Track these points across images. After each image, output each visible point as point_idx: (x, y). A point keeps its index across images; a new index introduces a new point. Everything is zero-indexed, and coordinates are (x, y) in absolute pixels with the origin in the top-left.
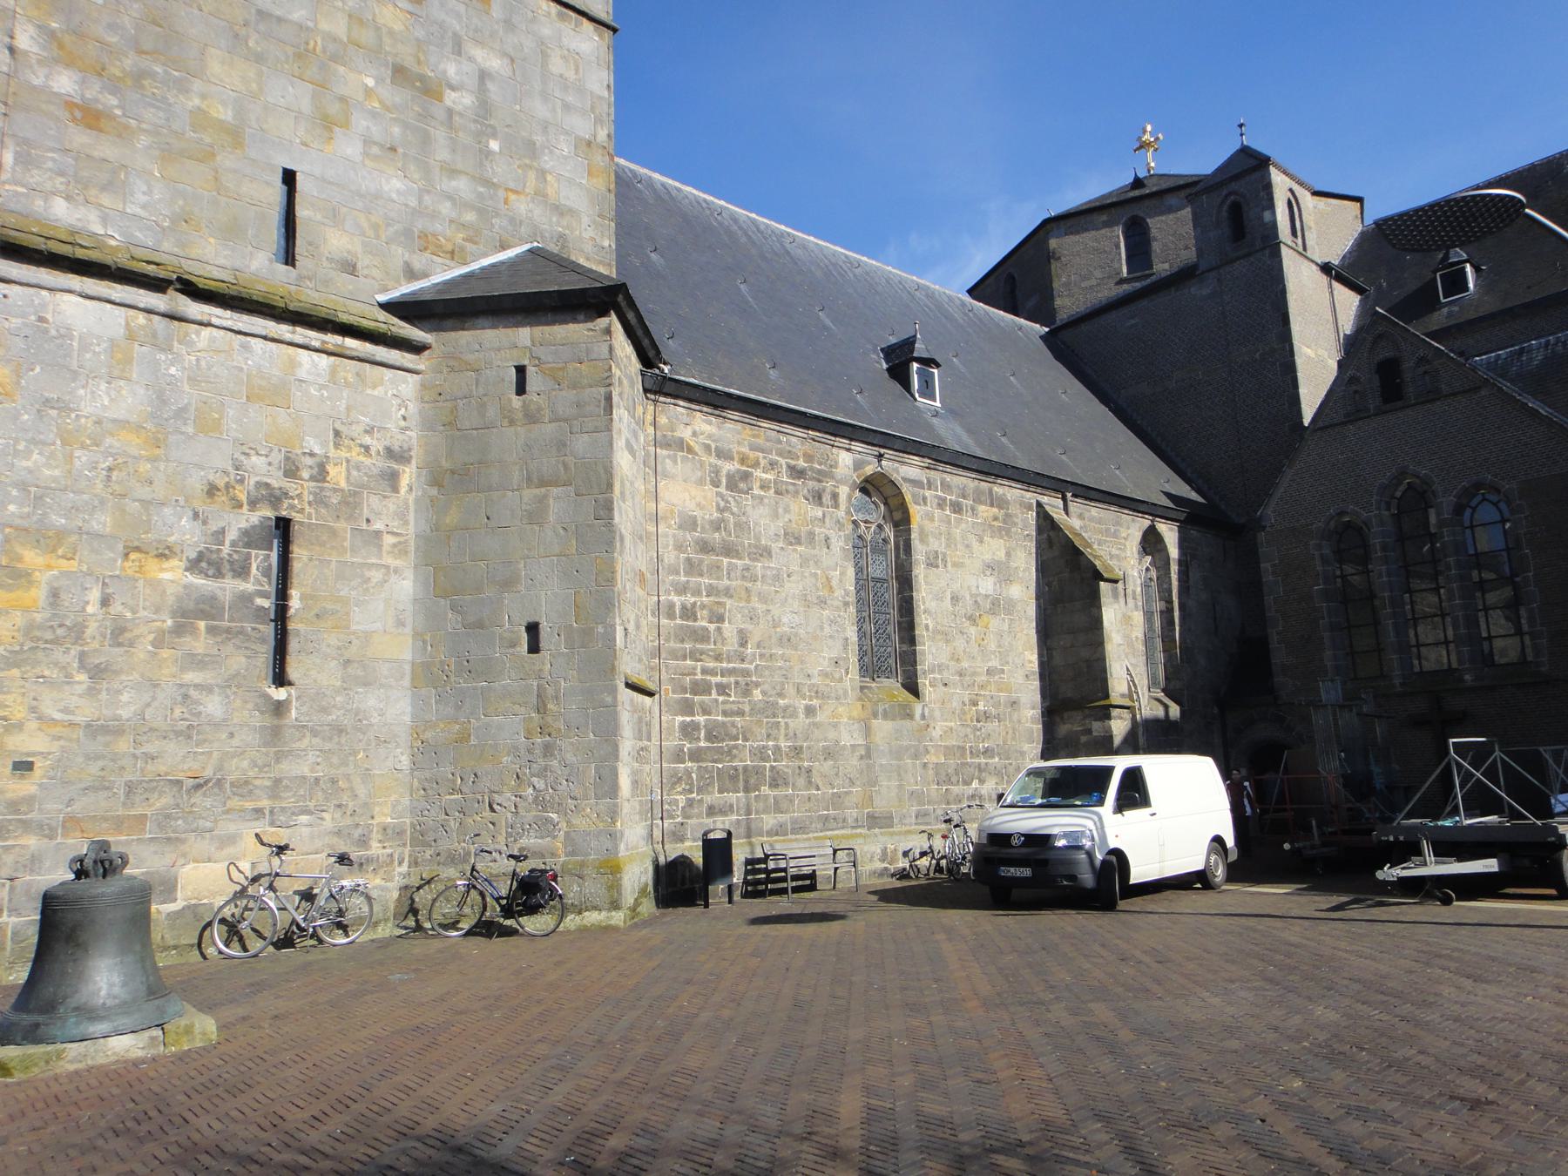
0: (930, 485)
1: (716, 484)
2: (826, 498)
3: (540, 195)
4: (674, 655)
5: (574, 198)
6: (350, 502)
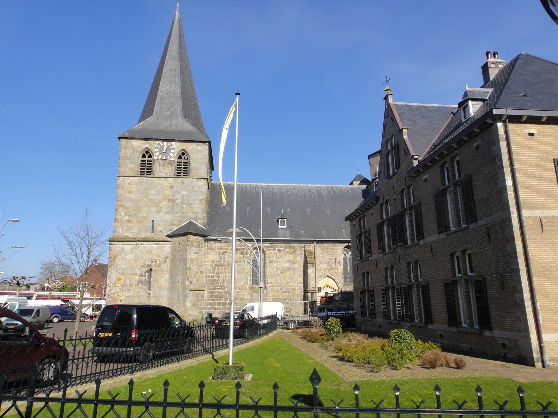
0: (271, 247)
1: (219, 254)
2: (245, 253)
3: (192, 211)
4: (209, 284)
5: (198, 210)
6: (160, 265)
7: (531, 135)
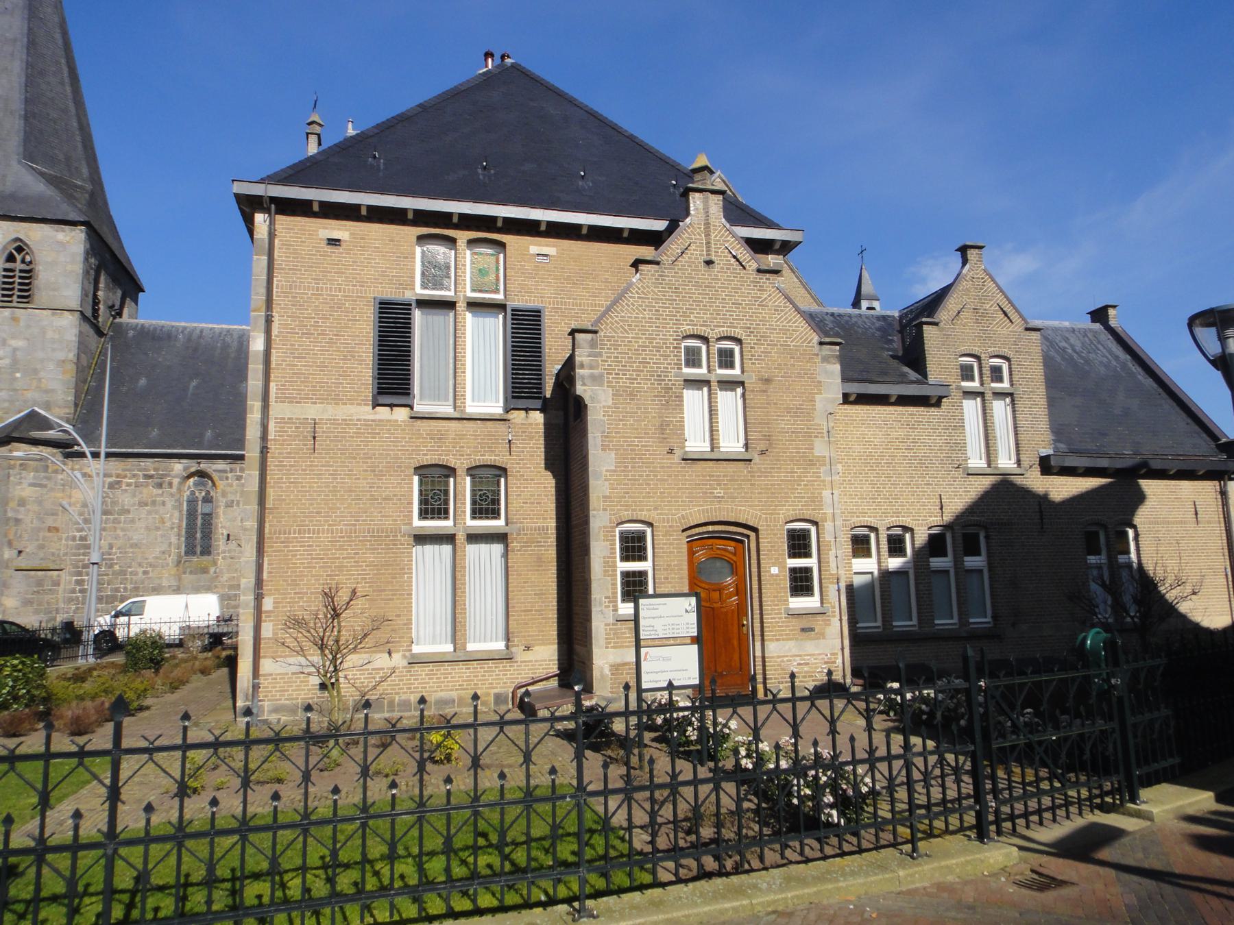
7: (334, 242)
